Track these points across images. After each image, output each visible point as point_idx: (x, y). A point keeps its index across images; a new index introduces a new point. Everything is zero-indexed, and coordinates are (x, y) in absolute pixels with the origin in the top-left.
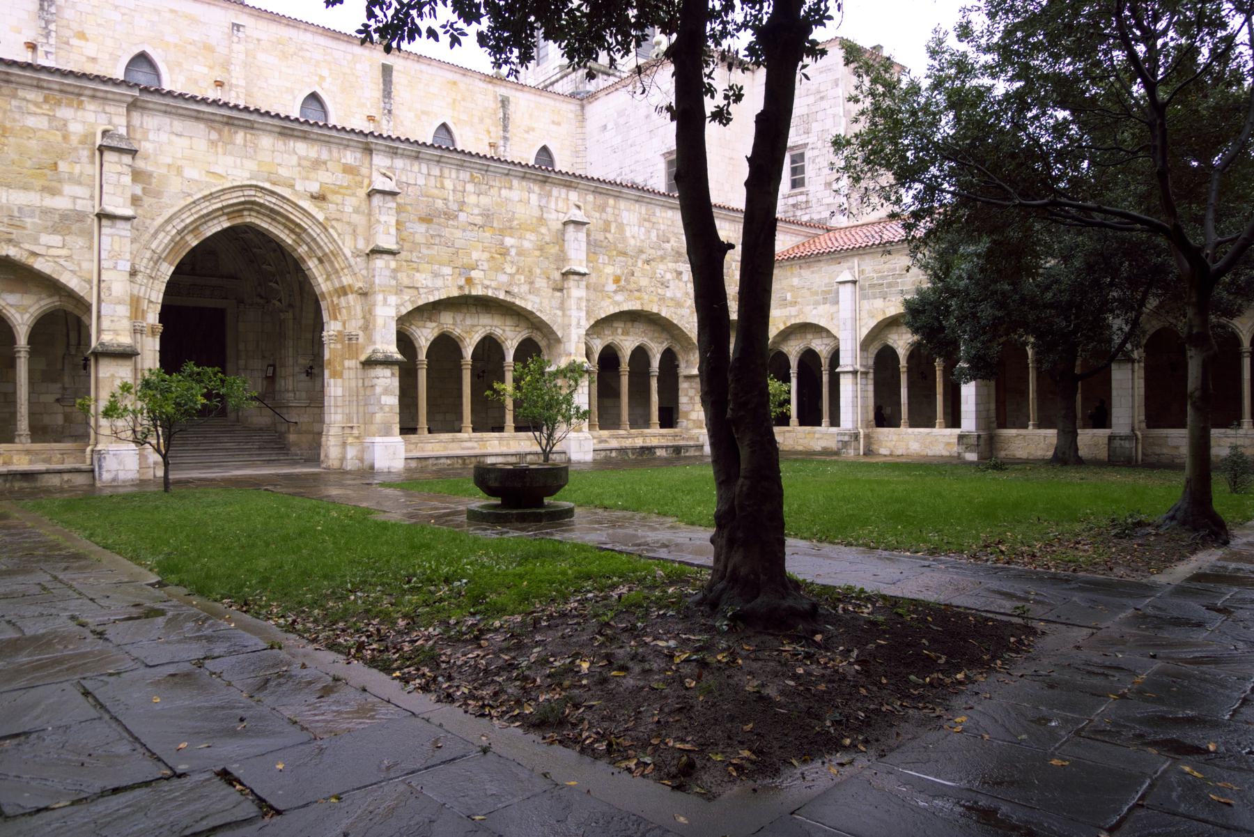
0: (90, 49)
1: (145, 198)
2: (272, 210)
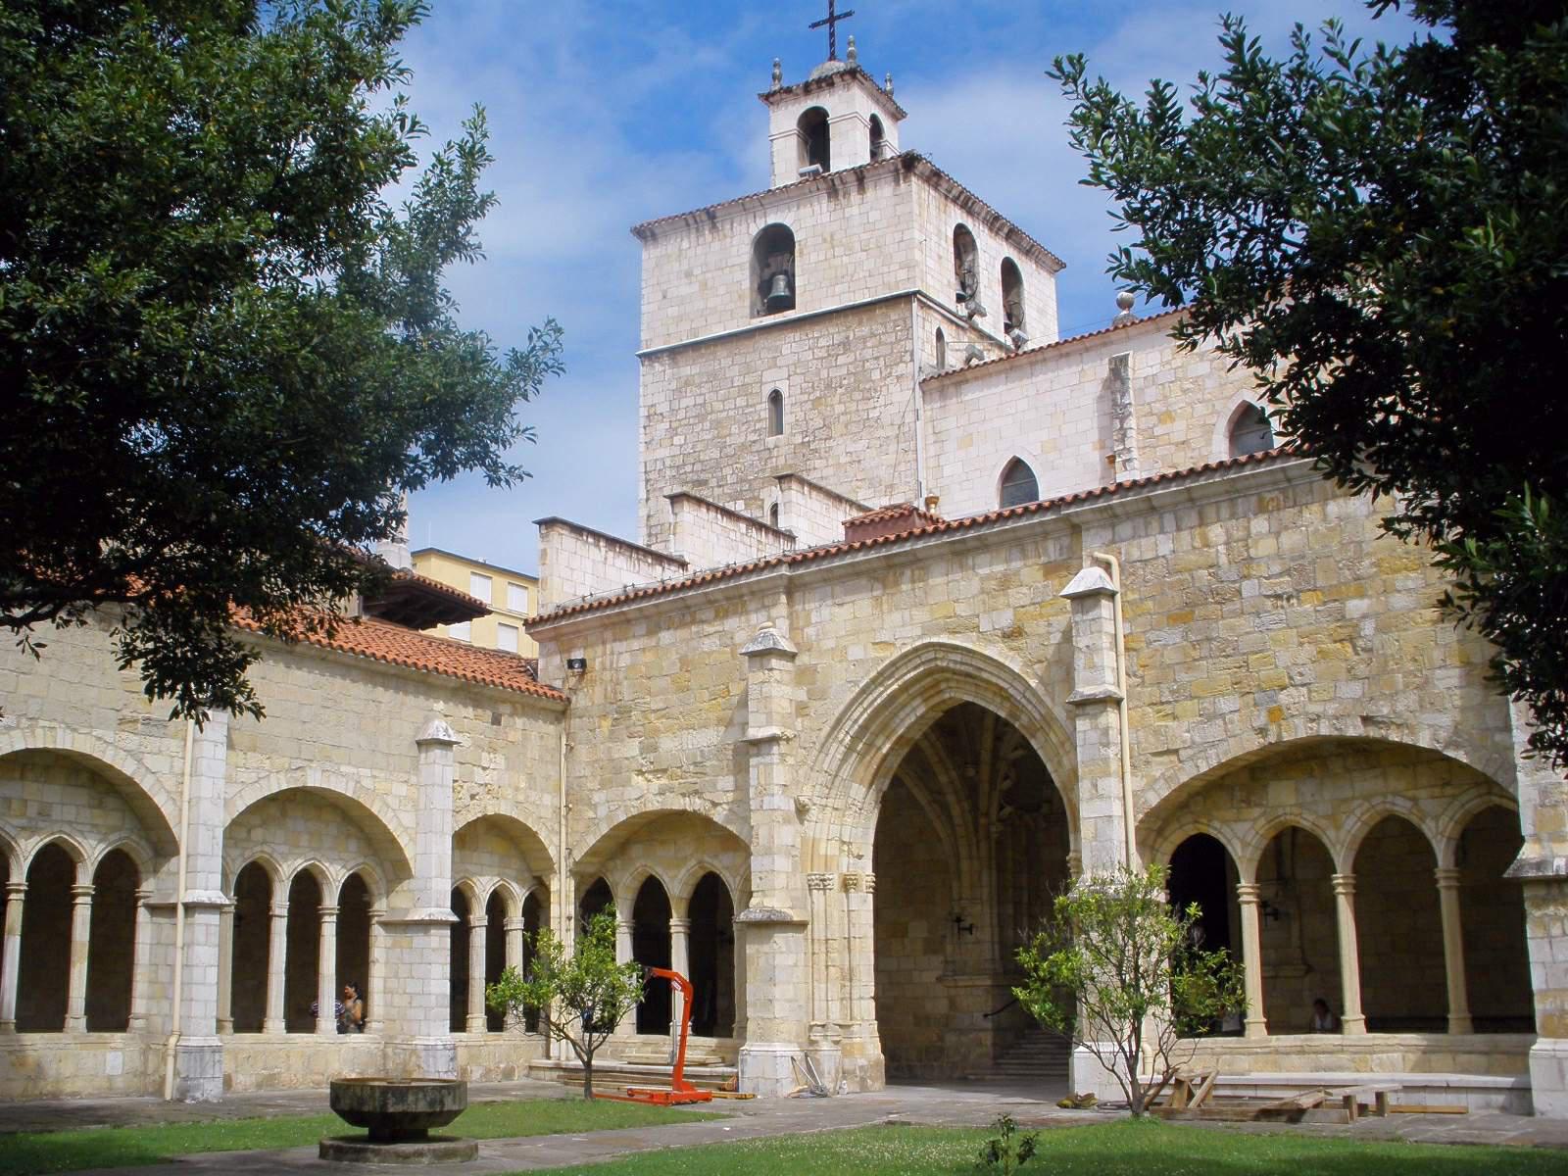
0: (1178, 429)
2: (968, 675)
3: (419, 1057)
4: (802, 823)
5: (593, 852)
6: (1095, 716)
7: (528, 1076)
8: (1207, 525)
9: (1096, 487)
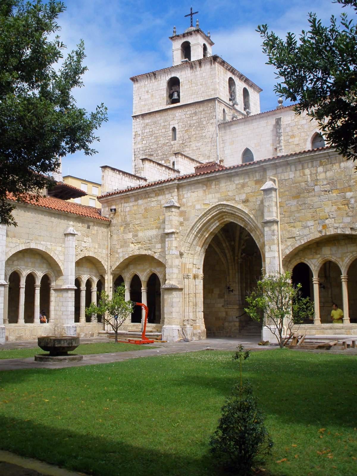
0: (296, 140)
1: (185, 222)
2: (232, 214)
3: (65, 330)
4: (181, 258)
5: (118, 267)
6: (270, 227)
7: (98, 336)
8: (304, 169)
9: (271, 157)
